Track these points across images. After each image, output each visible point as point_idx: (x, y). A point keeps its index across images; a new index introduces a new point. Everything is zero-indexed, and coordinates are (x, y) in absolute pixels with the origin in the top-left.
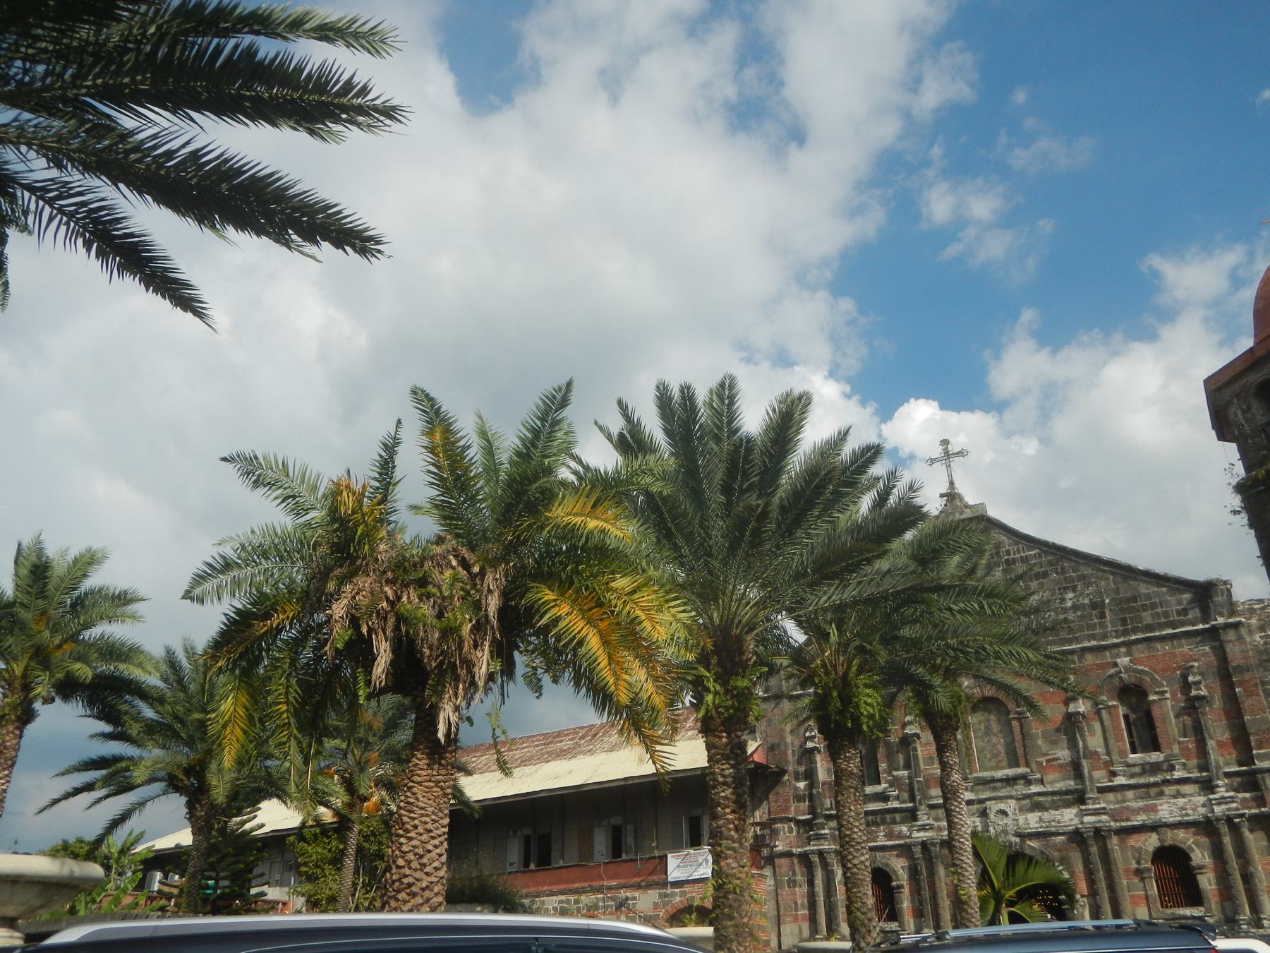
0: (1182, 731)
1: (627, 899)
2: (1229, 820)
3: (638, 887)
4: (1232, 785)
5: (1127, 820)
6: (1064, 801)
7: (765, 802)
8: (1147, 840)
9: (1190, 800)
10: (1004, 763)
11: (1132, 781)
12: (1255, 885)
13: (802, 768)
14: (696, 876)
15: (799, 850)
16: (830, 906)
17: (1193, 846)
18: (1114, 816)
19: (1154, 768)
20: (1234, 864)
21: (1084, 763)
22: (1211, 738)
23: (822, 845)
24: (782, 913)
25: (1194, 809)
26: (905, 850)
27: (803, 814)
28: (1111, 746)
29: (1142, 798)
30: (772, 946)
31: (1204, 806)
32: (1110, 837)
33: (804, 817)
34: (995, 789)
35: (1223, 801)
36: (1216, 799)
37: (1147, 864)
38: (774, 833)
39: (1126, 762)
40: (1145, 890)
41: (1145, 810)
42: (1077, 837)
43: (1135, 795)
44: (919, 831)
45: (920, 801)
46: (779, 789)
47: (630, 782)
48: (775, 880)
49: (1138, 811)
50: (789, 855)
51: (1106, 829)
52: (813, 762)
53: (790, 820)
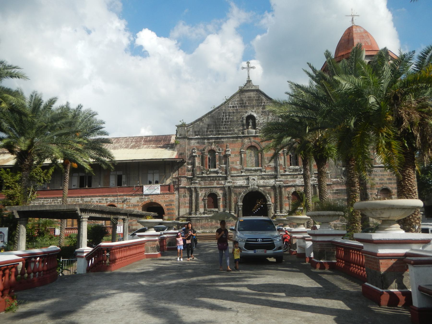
1: (127, 199)
3: (131, 195)
5: (288, 184)
6: (271, 177)
7: (177, 171)
10: (254, 165)
11: (290, 173)
14: (154, 193)
18: (284, 182)
19: (296, 170)
21: (279, 167)
24: (180, 205)
26: (223, 188)
27: (189, 176)
33: (190, 177)
34: (251, 172)
37: (290, 196)
41: (292, 181)
42: (274, 187)
44: (228, 183)
45: (229, 174)
46: (183, 167)
48: (179, 195)
49: (290, 181)
50: (185, 188)
52: (194, 160)
53: (186, 177)
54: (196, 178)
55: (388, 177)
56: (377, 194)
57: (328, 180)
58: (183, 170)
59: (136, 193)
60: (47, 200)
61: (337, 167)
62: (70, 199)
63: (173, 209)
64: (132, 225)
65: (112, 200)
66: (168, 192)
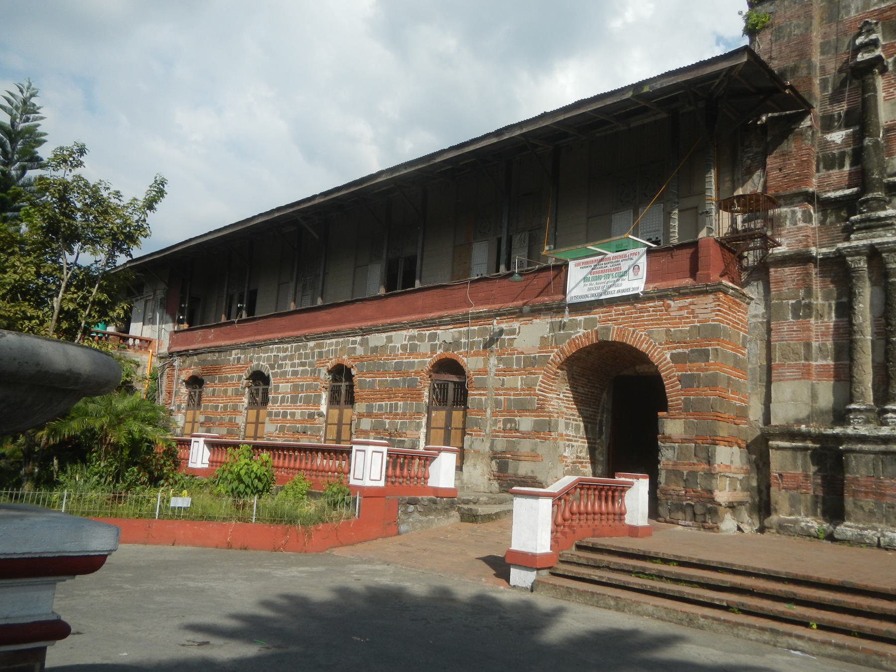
1: (501, 332)
3: (518, 314)
7: (759, 172)
13: (842, 108)
14: (614, 292)
15: (824, 250)
16: (887, 352)
23: (880, 236)
24: (776, 362)
30: (752, 418)
38: (775, 223)
46: (790, 145)
47: (506, 137)
48: (768, 306)
50: (801, 259)
53: (809, 198)
54: (879, 194)
58: (794, 162)
59: (539, 299)
60: (285, 346)
62: (334, 340)
63: (712, 382)
64: (517, 458)
65: (449, 340)
66: (688, 281)
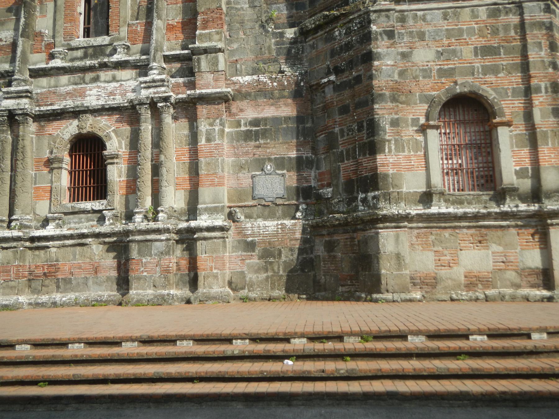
0: (136, 14)
2: (153, 104)
4: (170, 71)
5: (51, 105)
8: (67, 127)
9: (121, 85)
12: (162, 175)
17: (113, 134)
19: (99, 50)
20: (147, 152)
22: (159, 17)
25: (123, 95)
28: (57, 27)
29: (76, 84)
31: (134, 91)
32: (25, 122)
35: (154, 84)
36: (146, 82)
39: (68, 44)
40: (52, 182)
43: (69, 81)
51: (20, 112)
55: (482, 42)
56: (422, 121)
57: (216, 80)
61: (263, 26)
